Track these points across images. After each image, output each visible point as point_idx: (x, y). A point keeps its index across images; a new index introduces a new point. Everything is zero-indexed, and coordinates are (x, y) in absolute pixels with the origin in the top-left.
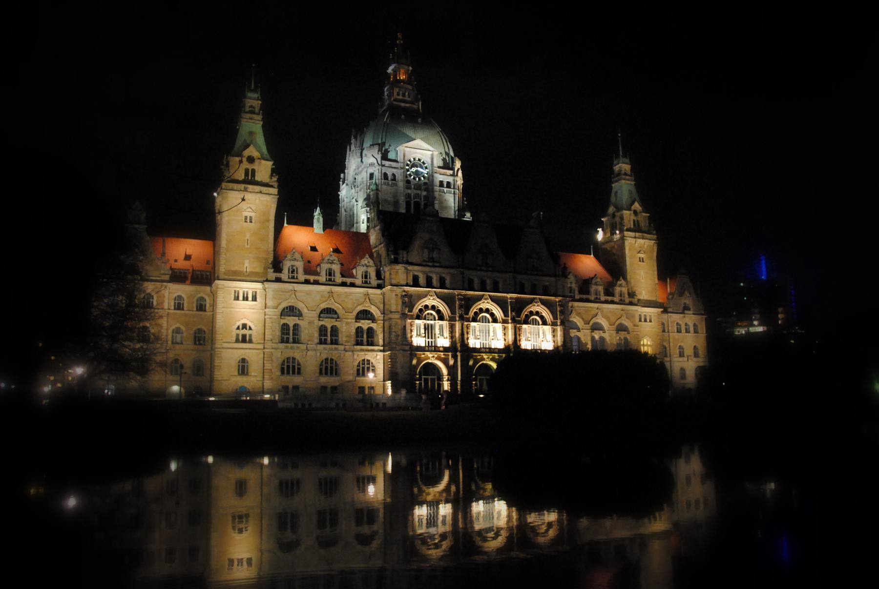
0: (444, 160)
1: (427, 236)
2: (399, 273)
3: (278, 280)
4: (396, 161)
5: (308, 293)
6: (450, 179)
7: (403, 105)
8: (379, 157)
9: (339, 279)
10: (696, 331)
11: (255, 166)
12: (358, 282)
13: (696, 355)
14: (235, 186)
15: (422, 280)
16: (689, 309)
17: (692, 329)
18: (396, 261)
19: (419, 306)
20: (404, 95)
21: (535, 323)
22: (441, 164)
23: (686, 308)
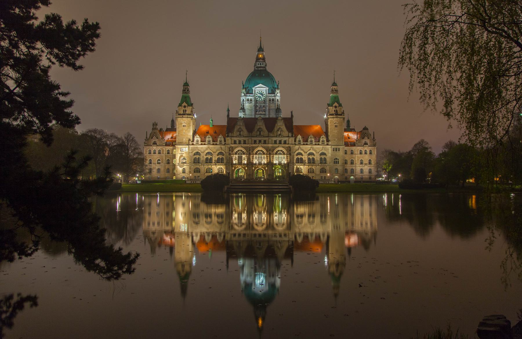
0: (272, 90)
1: (239, 127)
2: (229, 140)
3: (193, 144)
4: (252, 94)
5: (202, 148)
6: (274, 98)
7: (259, 69)
8: (245, 93)
9: (212, 143)
10: (371, 153)
11: (186, 109)
12: (218, 143)
13: (370, 163)
14: (180, 116)
15: (237, 142)
16: (367, 144)
17: (368, 153)
18: (228, 136)
19: (236, 150)
20: (261, 64)
21: (280, 154)
22: (270, 92)
23: (366, 144)
